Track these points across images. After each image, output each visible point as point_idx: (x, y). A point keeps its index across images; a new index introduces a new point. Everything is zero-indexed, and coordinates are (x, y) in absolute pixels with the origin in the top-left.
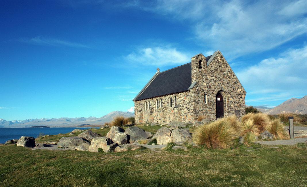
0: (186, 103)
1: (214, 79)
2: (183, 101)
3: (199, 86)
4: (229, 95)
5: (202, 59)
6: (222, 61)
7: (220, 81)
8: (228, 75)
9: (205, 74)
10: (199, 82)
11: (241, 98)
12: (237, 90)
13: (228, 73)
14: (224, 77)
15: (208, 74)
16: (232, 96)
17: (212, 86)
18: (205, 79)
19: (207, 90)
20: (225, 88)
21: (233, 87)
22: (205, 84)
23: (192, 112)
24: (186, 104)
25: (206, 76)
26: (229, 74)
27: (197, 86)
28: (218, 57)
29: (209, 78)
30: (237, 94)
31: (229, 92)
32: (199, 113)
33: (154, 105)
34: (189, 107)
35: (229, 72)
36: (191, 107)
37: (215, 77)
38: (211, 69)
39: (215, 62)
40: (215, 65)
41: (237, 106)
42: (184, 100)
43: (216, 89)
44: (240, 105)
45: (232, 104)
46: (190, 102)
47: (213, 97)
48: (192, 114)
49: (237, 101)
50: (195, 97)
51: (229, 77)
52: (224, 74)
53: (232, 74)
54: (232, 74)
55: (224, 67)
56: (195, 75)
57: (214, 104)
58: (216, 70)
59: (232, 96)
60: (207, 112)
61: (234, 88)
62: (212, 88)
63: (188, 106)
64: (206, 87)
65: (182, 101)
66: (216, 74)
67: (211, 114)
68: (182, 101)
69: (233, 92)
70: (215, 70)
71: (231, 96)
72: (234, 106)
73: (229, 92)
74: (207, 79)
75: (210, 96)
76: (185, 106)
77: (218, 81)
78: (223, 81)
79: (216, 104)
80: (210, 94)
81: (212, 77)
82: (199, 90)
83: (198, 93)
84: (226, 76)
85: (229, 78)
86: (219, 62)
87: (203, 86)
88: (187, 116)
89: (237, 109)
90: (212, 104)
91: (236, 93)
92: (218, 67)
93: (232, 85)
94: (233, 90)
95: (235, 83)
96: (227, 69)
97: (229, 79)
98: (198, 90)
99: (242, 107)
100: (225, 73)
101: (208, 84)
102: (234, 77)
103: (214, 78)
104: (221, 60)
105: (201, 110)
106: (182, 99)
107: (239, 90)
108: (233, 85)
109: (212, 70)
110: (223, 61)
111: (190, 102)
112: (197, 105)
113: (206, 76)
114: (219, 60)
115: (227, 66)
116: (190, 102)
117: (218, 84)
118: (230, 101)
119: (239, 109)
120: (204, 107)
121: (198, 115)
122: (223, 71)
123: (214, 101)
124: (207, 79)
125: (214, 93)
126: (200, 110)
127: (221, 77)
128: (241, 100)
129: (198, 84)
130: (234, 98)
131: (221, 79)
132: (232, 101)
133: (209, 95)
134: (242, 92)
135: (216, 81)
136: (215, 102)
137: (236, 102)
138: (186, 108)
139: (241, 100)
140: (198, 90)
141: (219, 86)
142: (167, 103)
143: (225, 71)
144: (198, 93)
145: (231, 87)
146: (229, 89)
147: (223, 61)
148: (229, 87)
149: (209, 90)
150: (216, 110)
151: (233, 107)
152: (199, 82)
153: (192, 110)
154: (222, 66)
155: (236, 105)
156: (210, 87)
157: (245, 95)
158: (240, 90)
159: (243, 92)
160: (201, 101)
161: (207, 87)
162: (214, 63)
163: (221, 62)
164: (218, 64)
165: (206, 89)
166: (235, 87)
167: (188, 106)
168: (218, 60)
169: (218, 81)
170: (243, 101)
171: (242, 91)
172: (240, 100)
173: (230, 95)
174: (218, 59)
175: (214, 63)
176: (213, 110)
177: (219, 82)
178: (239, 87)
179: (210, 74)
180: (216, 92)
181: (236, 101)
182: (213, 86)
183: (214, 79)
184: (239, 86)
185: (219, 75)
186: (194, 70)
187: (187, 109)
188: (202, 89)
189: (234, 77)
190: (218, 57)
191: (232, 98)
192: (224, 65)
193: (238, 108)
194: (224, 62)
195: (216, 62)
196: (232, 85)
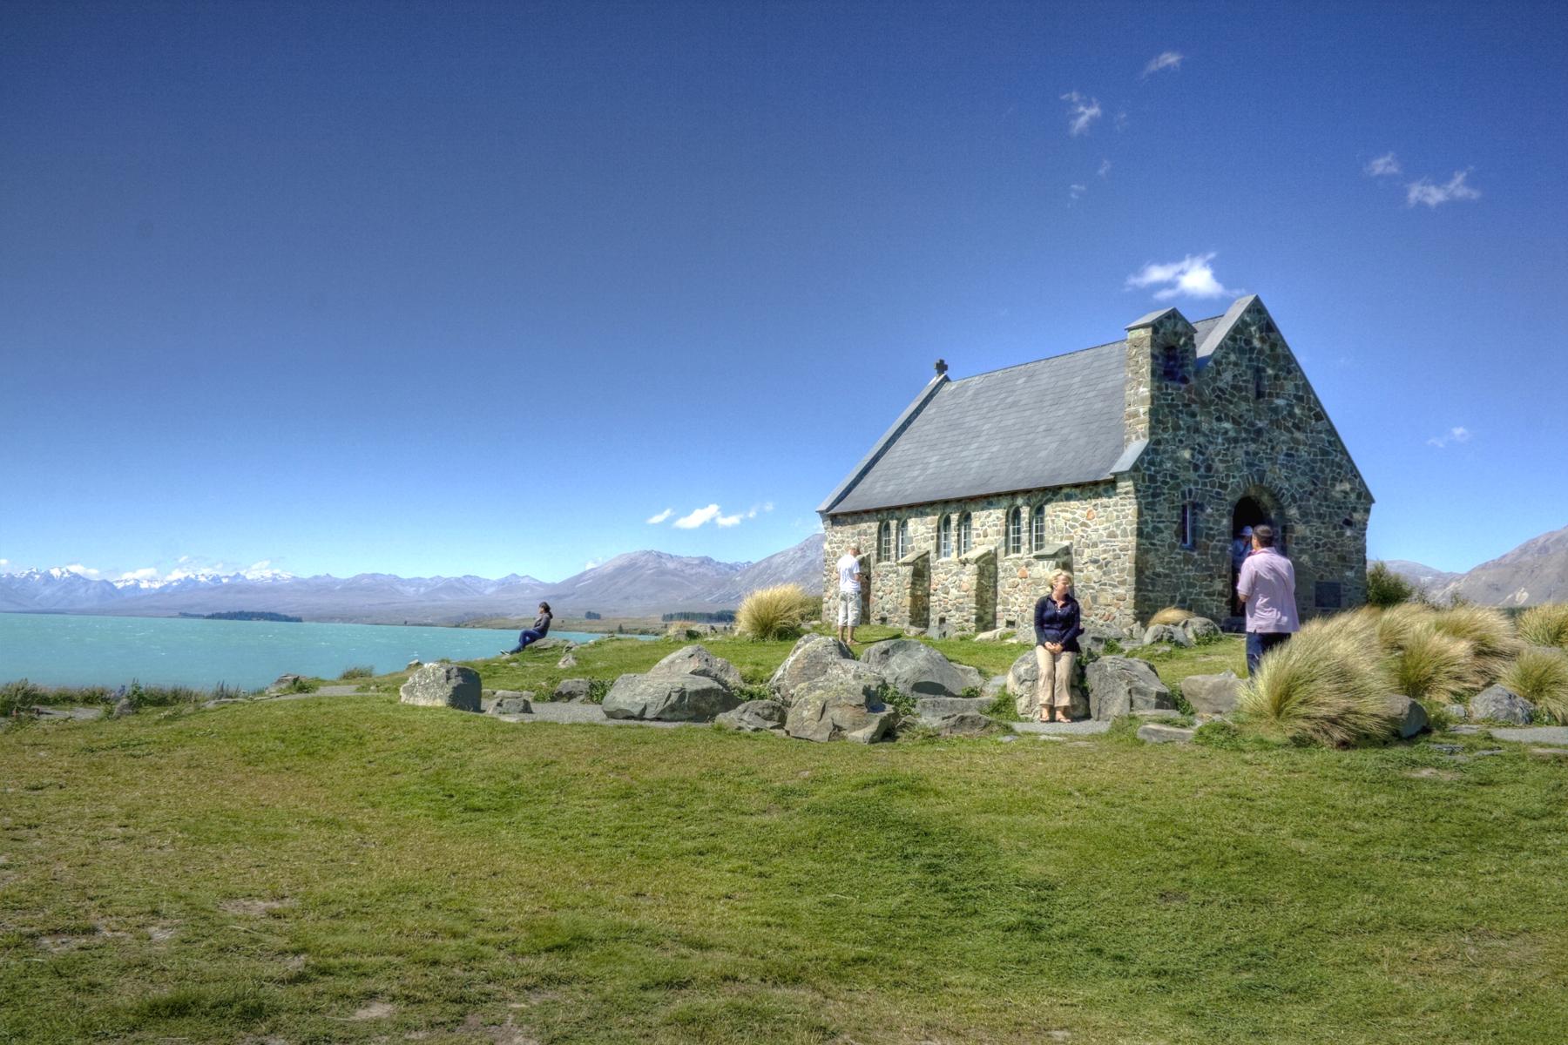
0: (1094, 537)
1: (1226, 432)
2: (1079, 529)
3: (1161, 462)
5: (1176, 334)
6: (1266, 348)
7: (1254, 441)
8: (1291, 415)
9: (1187, 405)
10: (1158, 442)
11: (1348, 523)
12: (1333, 486)
13: (1292, 406)
14: (1272, 422)
15: (1204, 404)
16: (1305, 516)
17: (1219, 466)
18: (1188, 428)
19: (1196, 483)
20: (1277, 475)
21: (1312, 470)
22: (1187, 454)
23: (1123, 583)
24: (1095, 545)
25: (1193, 415)
26: (1297, 411)
27: (1152, 463)
28: (1253, 329)
29: (1205, 427)
31: (1293, 496)
32: (1154, 585)
33: (926, 540)
34: (1109, 556)
35: (1300, 399)
36: (1117, 557)
37: (1235, 422)
38: (1214, 380)
39: (1233, 350)
40: (1236, 364)
41: (1327, 564)
42: (1084, 524)
44: (1343, 558)
46: (1115, 536)
47: (1222, 516)
48: (1121, 591)
50: (1140, 514)
52: (1275, 410)
54: (1310, 409)
55: (1276, 377)
56: (1142, 410)
57: (1223, 549)
58: (1240, 389)
60: (1190, 585)
61: (1317, 477)
63: (1105, 551)
65: (1073, 527)
66: (1236, 405)
67: (1207, 594)
68: (1073, 527)
70: (1234, 387)
73: (1293, 496)
74: (1197, 430)
75: (1209, 511)
76: (1087, 551)
77: (1244, 440)
80: (1209, 503)
81: (1219, 419)
82: (1159, 478)
83: (1154, 495)
85: (1298, 429)
86: (1252, 350)
87: (1176, 460)
88: (1094, 599)
89: (1329, 578)
90: (1215, 547)
95: (1325, 453)
96: (1289, 387)
97: (1298, 435)
98: (1152, 479)
100: (1280, 402)
101: (1200, 453)
102: (1320, 425)
103: (1227, 425)
104: (1262, 340)
105: (1166, 576)
106: (1075, 520)
107: (1339, 487)
109: (1220, 390)
110: (1273, 346)
111: (1112, 535)
112: (1147, 551)
113: (1193, 415)
114: (1256, 343)
115: (1289, 372)
116: (1112, 535)
117: (1247, 453)
119: (1335, 578)
120: (1178, 562)
121: (1151, 595)
122: (1270, 395)
123: (1222, 534)
124: (1197, 430)
126: (1158, 575)
128: (1348, 533)
129: (1155, 451)
130: (1316, 523)
131: (1259, 432)
132: (1304, 538)
133: (1203, 510)
134: (1353, 496)
135: (1236, 440)
138: (1096, 562)
139: (1348, 533)
140: (1152, 479)
141: (1250, 465)
142: (998, 533)
143: (1278, 396)
144: (1154, 495)
145: (1304, 474)
146: (1295, 481)
147: (1273, 346)
148: (1293, 468)
149: (1205, 484)
151: (1310, 564)
152: (1158, 442)
153: (1122, 571)
154: (1270, 371)
156: (1209, 468)
157: (1367, 511)
158: (1347, 486)
159: (1359, 496)
160: (1166, 534)
161: (1196, 468)
162: (1233, 357)
163: (1261, 352)
164: (1250, 360)
165: (1192, 475)
166: (1322, 471)
167: (1105, 551)
168: (1248, 342)
169: (1244, 440)
170: (1355, 539)
171: (1352, 490)
172: (1341, 535)
173: (1299, 508)
175: (1233, 357)
177: (1253, 447)
180: (1234, 491)
182: (1221, 461)
183: (1226, 432)
184: (1340, 466)
186: (1140, 384)
187: (1100, 567)
188: (1172, 477)
191: (1307, 522)
192: (1273, 367)
194: (1279, 350)
195: (1241, 351)
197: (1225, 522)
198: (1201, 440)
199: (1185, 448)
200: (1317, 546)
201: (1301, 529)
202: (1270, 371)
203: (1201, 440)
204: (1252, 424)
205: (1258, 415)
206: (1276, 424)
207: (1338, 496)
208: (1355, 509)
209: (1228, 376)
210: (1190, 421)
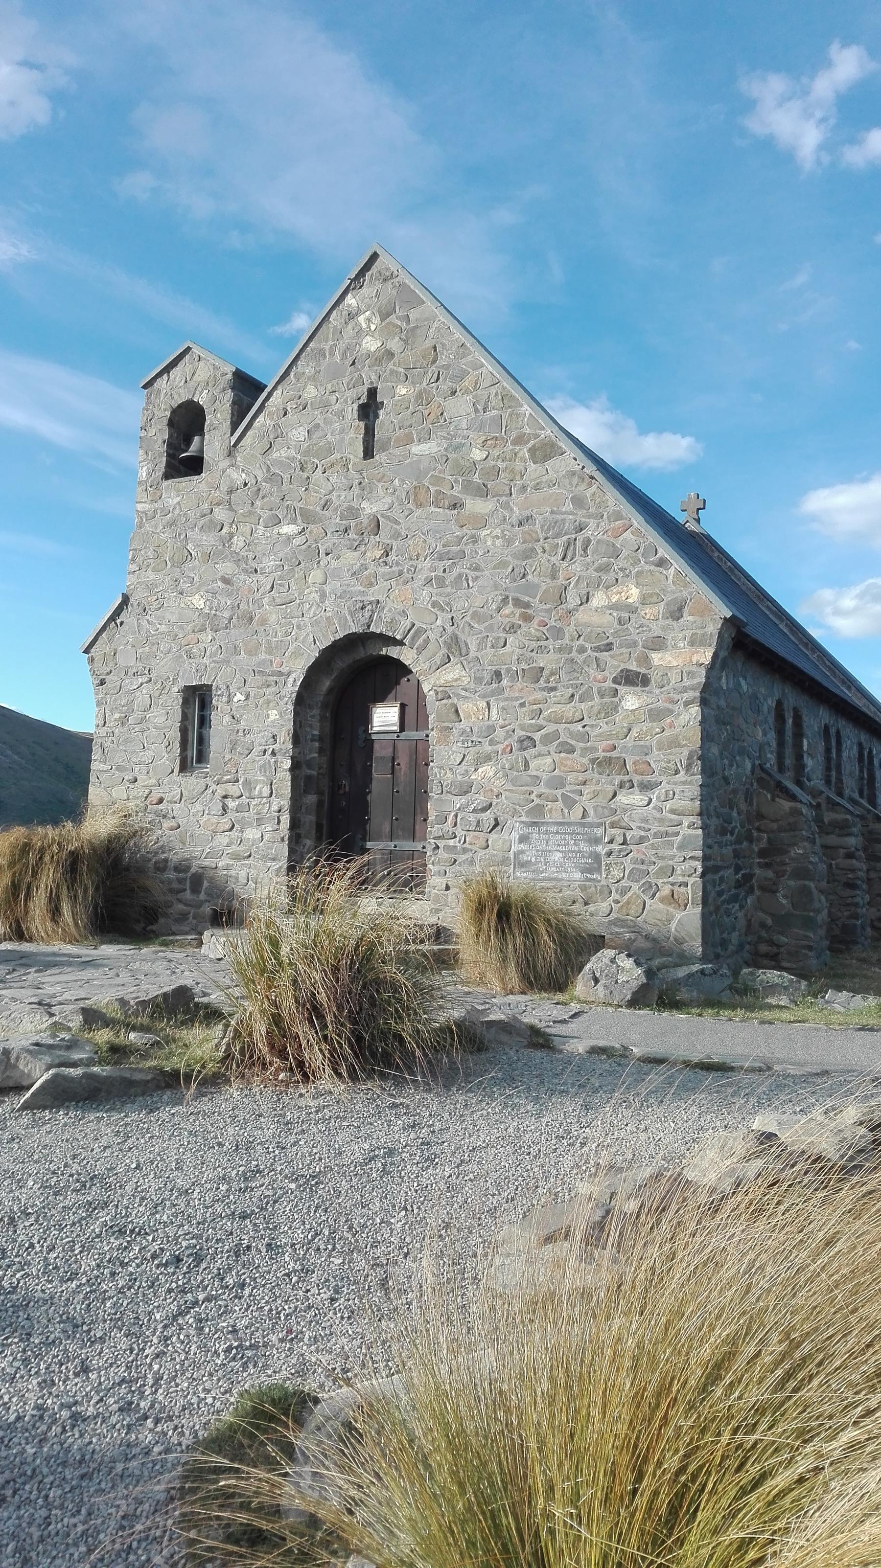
4: (452, 674)
26: (478, 454)
28: (361, 319)
30: (560, 650)
37: (308, 517)
39: (314, 378)
43: (303, 634)
44: (609, 764)
45: (488, 758)
49: (557, 720)
51: (468, 487)
53: (520, 440)
59: (498, 675)
61: (530, 589)
62: (263, 622)
64: (203, 629)
69: (513, 629)
70: (307, 453)
71: (478, 680)
72: (514, 782)
75: (239, 697)
78: (396, 535)
79: (288, 764)
84: (437, 480)
85: (483, 492)
91: (558, 633)
92: (352, 411)
93: (503, 564)
94: (517, 603)
99: (646, 787)
103: (288, 529)
104: (387, 331)
107: (599, 599)
108: (529, 554)
118: (464, 732)
125: (284, 669)
127: (369, 508)
128: (631, 700)
136: (277, 747)
137: (556, 735)
143: (427, 437)
150: (286, 819)
155: (541, 765)
158: (634, 593)
170: (656, 715)
171: (645, 600)
174: (360, 333)
175: (311, 392)
176: (260, 821)
177: (350, 557)
178: (604, 569)
179: (258, 503)
180: (297, 654)
181: (551, 728)
185: (356, 490)
189: (549, 464)
190: (352, 316)
193: (570, 803)
196: (503, 564)
197: (274, 714)
198: (226, 568)
199: (198, 590)
200: (527, 742)
201: (471, 708)
202: (402, 390)
203: (226, 568)
204: (353, 513)
205: (365, 489)
206: (417, 498)
207: (608, 620)
208: (658, 644)
209: (299, 434)
210: (209, 540)
